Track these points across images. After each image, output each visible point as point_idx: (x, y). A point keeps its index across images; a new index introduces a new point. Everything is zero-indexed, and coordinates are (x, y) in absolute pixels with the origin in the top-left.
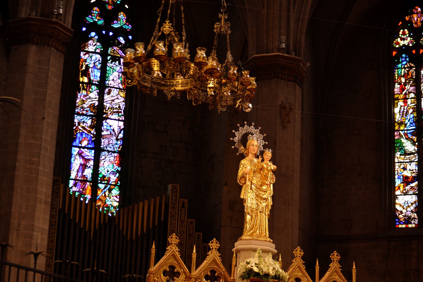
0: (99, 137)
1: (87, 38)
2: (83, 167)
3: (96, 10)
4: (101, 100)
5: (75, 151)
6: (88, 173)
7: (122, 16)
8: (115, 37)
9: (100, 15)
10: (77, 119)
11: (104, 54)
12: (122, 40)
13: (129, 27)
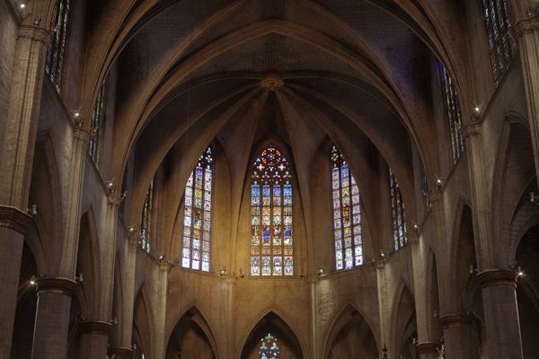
3: (264, 344)
7: (274, 344)
9: (266, 346)
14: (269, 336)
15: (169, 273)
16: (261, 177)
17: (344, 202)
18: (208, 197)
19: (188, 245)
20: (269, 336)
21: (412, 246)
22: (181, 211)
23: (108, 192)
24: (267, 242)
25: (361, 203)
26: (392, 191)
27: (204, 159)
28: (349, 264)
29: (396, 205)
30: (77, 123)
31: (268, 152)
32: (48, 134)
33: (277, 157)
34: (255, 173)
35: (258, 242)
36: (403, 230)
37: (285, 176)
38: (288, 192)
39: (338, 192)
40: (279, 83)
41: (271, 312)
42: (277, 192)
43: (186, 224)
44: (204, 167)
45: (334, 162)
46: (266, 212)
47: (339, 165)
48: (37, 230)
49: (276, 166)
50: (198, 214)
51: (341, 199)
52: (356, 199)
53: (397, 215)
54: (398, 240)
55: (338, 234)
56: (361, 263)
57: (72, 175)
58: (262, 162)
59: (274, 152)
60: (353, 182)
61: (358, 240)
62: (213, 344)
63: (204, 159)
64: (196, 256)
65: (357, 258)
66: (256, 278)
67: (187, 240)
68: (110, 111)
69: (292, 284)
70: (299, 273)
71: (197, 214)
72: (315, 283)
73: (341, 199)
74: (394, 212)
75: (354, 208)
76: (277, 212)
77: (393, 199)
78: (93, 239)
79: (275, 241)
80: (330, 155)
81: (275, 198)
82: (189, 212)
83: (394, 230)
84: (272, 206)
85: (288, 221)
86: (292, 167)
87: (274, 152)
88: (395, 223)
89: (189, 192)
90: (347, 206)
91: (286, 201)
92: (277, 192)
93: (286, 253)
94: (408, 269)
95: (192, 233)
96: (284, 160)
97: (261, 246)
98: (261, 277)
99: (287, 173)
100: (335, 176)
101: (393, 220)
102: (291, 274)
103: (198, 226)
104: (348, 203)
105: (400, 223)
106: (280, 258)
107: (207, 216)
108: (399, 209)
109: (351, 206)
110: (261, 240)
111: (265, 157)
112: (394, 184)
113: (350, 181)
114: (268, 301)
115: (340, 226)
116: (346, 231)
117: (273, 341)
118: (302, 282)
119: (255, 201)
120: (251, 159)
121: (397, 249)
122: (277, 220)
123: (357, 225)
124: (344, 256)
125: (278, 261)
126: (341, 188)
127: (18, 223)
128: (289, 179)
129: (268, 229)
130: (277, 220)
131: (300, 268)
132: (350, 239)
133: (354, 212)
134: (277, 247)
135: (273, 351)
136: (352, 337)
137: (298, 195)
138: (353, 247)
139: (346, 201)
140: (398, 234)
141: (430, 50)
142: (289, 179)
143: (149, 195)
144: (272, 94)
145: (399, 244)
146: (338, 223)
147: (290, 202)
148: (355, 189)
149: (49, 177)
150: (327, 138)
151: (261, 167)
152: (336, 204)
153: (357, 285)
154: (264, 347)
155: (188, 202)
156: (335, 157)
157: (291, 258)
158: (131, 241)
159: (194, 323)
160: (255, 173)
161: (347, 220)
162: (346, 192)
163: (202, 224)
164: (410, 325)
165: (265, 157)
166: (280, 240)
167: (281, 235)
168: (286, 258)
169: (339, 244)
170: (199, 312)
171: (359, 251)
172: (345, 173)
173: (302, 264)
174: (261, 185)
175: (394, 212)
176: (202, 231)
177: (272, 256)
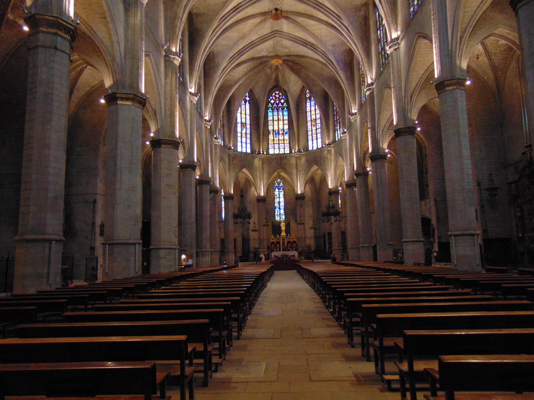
0: (280, 207)
1: (275, 189)
2: (278, 212)
3: (276, 183)
4: (279, 200)
5: (276, 210)
6: (279, 213)
7: (281, 183)
8: (281, 188)
9: (277, 184)
10: (275, 204)
11: (279, 191)
13: (283, 185)
14: (279, 180)
16: (272, 107)
17: (312, 117)
18: (248, 117)
20: (279, 180)
24: (277, 137)
25: (320, 118)
28: (315, 148)
33: (280, 96)
34: (270, 104)
36: (340, 131)
37: (284, 105)
38: (286, 113)
39: (310, 112)
40: (280, 61)
42: (281, 113)
44: (245, 102)
45: (308, 98)
46: (276, 123)
49: (280, 100)
50: (243, 125)
52: (318, 116)
53: (337, 124)
55: (310, 133)
59: (278, 94)
60: (317, 108)
65: (319, 145)
71: (244, 126)
74: (336, 123)
75: (317, 120)
76: (281, 123)
77: (335, 116)
80: (306, 94)
81: (279, 116)
82: (239, 125)
83: (336, 131)
84: (278, 120)
85: (286, 127)
86: (287, 101)
87: (278, 94)
90: (314, 120)
92: (281, 113)
93: (285, 142)
96: (283, 97)
97: (274, 140)
99: (285, 104)
100: (308, 105)
103: (244, 131)
105: (338, 128)
108: (338, 121)
109: (316, 120)
110: (274, 136)
111: (274, 96)
115: (310, 129)
116: (314, 132)
117: (280, 182)
119: (270, 118)
120: (268, 97)
121: (337, 140)
123: (318, 129)
124: (313, 143)
125: (282, 146)
126: (311, 111)
129: (277, 131)
130: (281, 127)
132: (315, 135)
134: (281, 140)
135: (281, 187)
139: (313, 117)
140: (338, 133)
142: (286, 107)
144: (277, 67)
152: (309, 119)
154: (277, 185)
155: (239, 120)
156: (308, 96)
157: (288, 144)
160: (270, 104)
162: (313, 112)
163: (246, 130)
165: (274, 96)
167: (283, 134)
168: (285, 145)
169: (310, 138)
172: (313, 103)
174: (273, 110)
175: (336, 123)
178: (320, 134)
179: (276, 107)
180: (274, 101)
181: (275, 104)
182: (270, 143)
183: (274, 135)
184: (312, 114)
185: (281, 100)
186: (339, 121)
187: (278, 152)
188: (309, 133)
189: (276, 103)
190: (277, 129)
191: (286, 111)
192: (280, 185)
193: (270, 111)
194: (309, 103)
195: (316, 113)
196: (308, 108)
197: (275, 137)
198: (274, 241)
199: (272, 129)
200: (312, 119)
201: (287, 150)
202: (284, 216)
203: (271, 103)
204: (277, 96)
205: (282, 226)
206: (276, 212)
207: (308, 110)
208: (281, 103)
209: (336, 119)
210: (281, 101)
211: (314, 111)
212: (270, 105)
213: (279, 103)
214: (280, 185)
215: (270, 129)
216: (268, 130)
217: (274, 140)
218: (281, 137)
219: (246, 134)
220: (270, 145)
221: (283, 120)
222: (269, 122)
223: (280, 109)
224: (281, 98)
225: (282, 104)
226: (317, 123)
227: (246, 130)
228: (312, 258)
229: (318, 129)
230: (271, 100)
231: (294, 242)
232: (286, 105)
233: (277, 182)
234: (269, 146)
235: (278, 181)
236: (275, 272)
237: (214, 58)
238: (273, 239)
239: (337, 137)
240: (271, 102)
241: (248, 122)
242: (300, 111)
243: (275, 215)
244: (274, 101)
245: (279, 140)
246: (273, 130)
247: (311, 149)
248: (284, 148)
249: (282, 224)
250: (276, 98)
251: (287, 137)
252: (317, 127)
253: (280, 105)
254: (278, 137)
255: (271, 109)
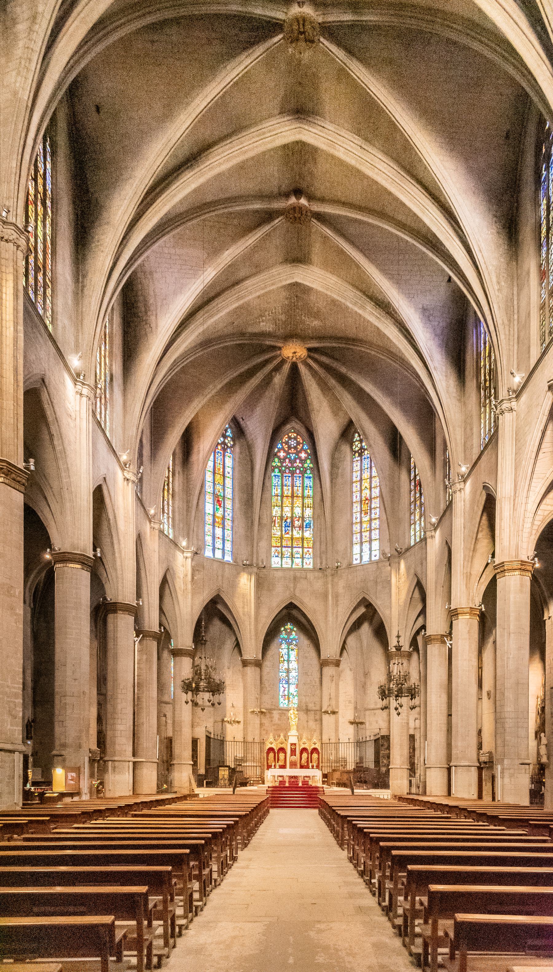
12: (294, 642)
13: (296, 637)
14: (289, 626)
15: (192, 560)
17: (363, 495)
18: (229, 482)
19: (211, 533)
20: (289, 626)
21: (429, 540)
22: (202, 495)
23: (123, 466)
24: (288, 533)
25: (381, 496)
26: (413, 484)
27: (224, 443)
28: (366, 558)
29: (415, 499)
30: (78, 375)
31: (290, 438)
32: (43, 380)
33: (298, 443)
34: (276, 460)
35: (279, 533)
36: (420, 524)
37: (306, 465)
39: (359, 483)
41: (291, 603)
42: (298, 483)
43: (207, 511)
44: (224, 450)
45: (355, 452)
46: (287, 501)
47: (360, 455)
48: (46, 498)
49: (298, 453)
50: (219, 501)
51: (361, 490)
52: (376, 492)
54: (415, 535)
55: (356, 528)
56: (377, 558)
57: (78, 438)
58: (283, 449)
59: (295, 438)
60: (374, 474)
61: (375, 534)
62: (237, 632)
63: (224, 443)
64: (219, 544)
65: (374, 553)
66: (277, 570)
67: (208, 528)
68: (117, 369)
69: (310, 576)
70: (319, 566)
72: (332, 575)
73: (361, 490)
74: (413, 506)
75: (373, 501)
76: (298, 502)
77: (413, 493)
78: (111, 517)
79: (295, 533)
80: (351, 444)
81: (295, 488)
82: (209, 499)
83: (411, 525)
84: (293, 496)
85: (308, 512)
87: (295, 438)
88: (413, 517)
89: (209, 477)
90: (367, 499)
91: (306, 493)
92: (298, 483)
93: (305, 545)
94: (422, 564)
95: (214, 521)
97: (282, 538)
98: (282, 569)
99: (308, 461)
100: (357, 466)
101: (411, 514)
102: (311, 567)
103: (219, 513)
104: (368, 496)
105: (417, 517)
106: (300, 550)
107: (229, 504)
108: (418, 503)
109: (371, 499)
110: (282, 531)
111: (287, 443)
112: (415, 476)
113: (371, 472)
114: (288, 593)
115: (358, 520)
116: (364, 525)
118: (320, 574)
119: (276, 491)
122: (298, 511)
123: (375, 519)
124: (361, 551)
125: (298, 553)
126: (361, 480)
127: (14, 479)
128: (311, 469)
129: (289, 520)
130: (298, 511)
131: (318, 561)
132: (367, 534)
133: (373, 506)
135: (292, 640)
136: (366, 629)
137: (318, 481)
138: (370, 541)
139: (366, 493)
140: (415, 529)
141: (468, 300)
142: (311, 469)
143: (168, 477)
145: (415, 540)
146: (356, 516)
147: (311, 493)
148: (376, 482)
149: (51, 436)
150: (350, 423)
151: (282, 454)
152: (356, 497)
153: (372, 578)
155: (209, 488)
157: (311, 550)
158: (152, 525)
159: (219, 610)
160: (276, 460)
161: (366, 513)
162: (366, 484)
163: (224, 511)
164: (422, 616)
165: (287, 443)
166: (300, 532)
168: (306, 550)
169: (357, 538)
170: (223, 599)
171: (376, 545)
172: (366, 463)
173: (321, 558)
175: (413, 506)
176: (224, 518)
177: (292, 547)
178: (377, 531)
179: (289, 468)
180: (285, 454)
181: (287, 460)
182: (274, 544)
183: (283, 529)
184: (363, 488)
185: (300, 452)
186: (421, 501)
187: (290, 563)
188: (354, 529)
189: (290, 457)
190: (289, 515)
191: (310, 478)
192: (292, 637)
193: (275, 476)
194: (359, 464)
195: (373, 486)
196: (355, 474)
197: (284, 532)
198: (273, 746)
199: (279, 514)
200: (364, 499)
201: (308, 563)
202: (296, 698)
203: (279, 458)
204: (293, 443)
205: (293, 716)
206: (282, 689)
207: (355, 479)
208: (300, 458)
209: (412, 499)
210: (300, 455)
211: (368, 480)
212: (276, 462)
213: (295, 459)
214: (292, 637)
215: (274, 514)
216: (272, 517)
217: (282, 538)
218: (297, 534)
219: (224, 518)
220: (273, 549)
221: (303, 497)
222: (274, 499)
223: (298, 471)
224: (299, 447)
225: (303, 461)
226: (373, 506)
227: (224, 511)
228: (351, 783)
229: (375, 519)
230: (279, 451)
231: (315, 750)
232: (311, 465)
233: (285, 630)
234: (271, 550)
235: (286, 627)
236: (271, 811)
237: (149, 313)
238: (271, 743)
239: (413, 538)
240: (279, 454)
241: (229, 493)
242: (340, 480)
243: (279, 694)
244: (285, 454)
245: (292, 539)
246: (282, 517)
247: (358, 561)
248: (303, 558)
249: (291, 712)
250: (290, 448)
251: (308, 534)
252: (373, 516)
253: (298, 463)
254: (290, 533)
255: (280, 471)
